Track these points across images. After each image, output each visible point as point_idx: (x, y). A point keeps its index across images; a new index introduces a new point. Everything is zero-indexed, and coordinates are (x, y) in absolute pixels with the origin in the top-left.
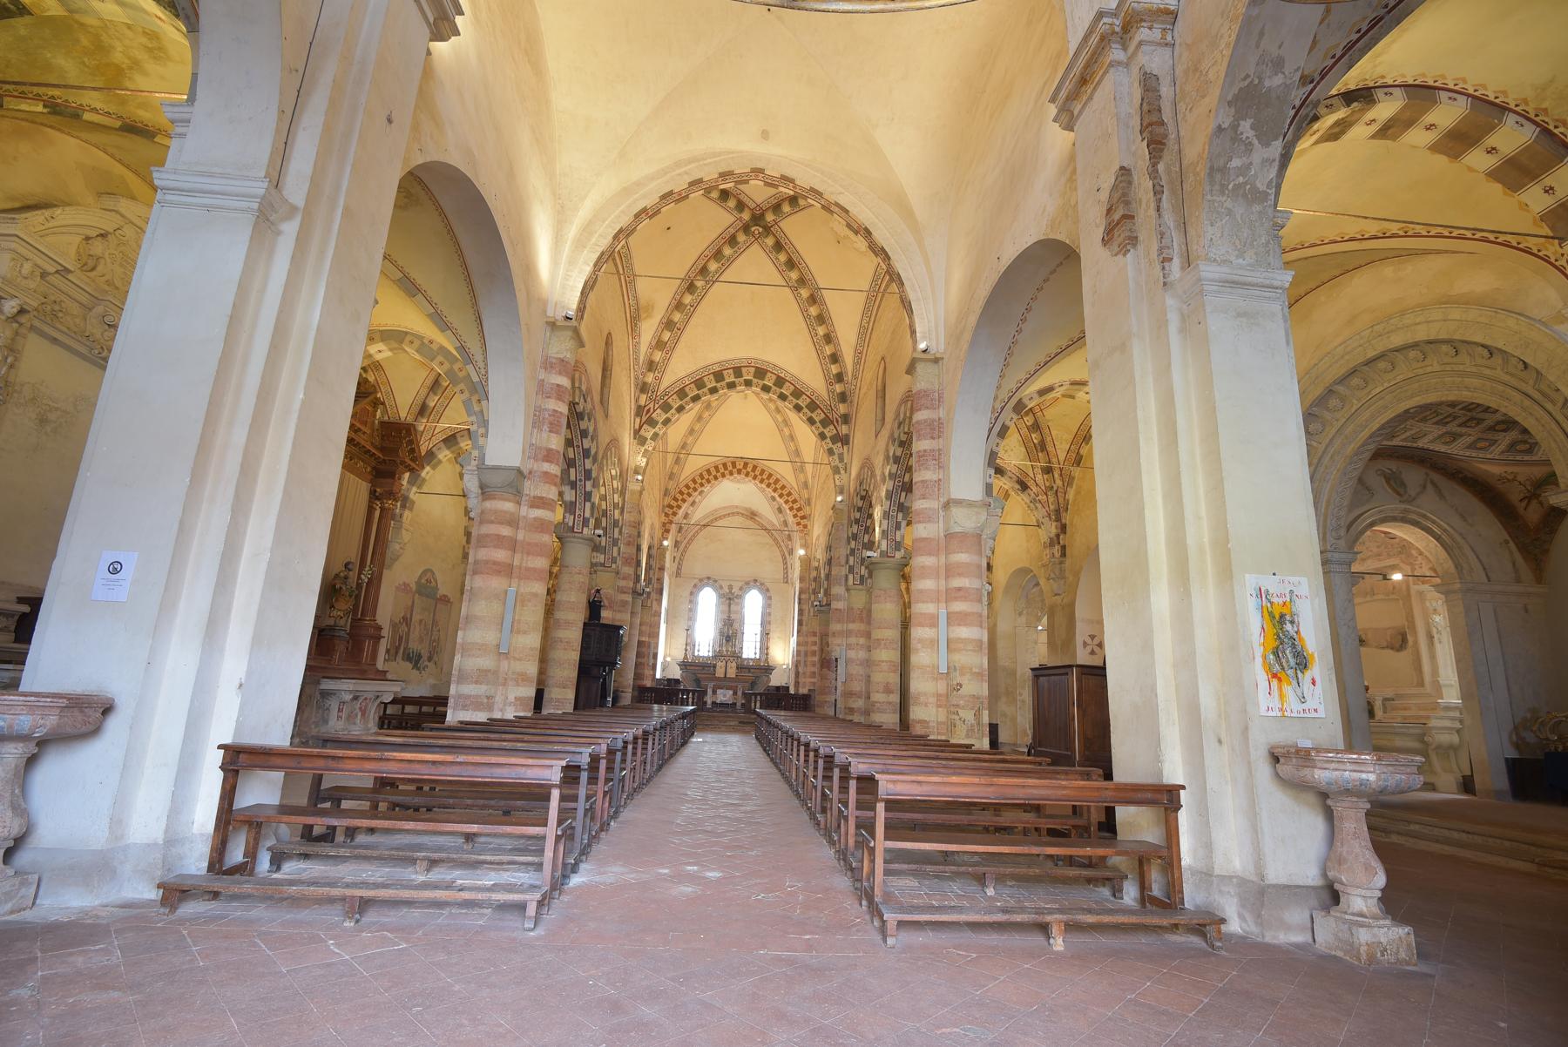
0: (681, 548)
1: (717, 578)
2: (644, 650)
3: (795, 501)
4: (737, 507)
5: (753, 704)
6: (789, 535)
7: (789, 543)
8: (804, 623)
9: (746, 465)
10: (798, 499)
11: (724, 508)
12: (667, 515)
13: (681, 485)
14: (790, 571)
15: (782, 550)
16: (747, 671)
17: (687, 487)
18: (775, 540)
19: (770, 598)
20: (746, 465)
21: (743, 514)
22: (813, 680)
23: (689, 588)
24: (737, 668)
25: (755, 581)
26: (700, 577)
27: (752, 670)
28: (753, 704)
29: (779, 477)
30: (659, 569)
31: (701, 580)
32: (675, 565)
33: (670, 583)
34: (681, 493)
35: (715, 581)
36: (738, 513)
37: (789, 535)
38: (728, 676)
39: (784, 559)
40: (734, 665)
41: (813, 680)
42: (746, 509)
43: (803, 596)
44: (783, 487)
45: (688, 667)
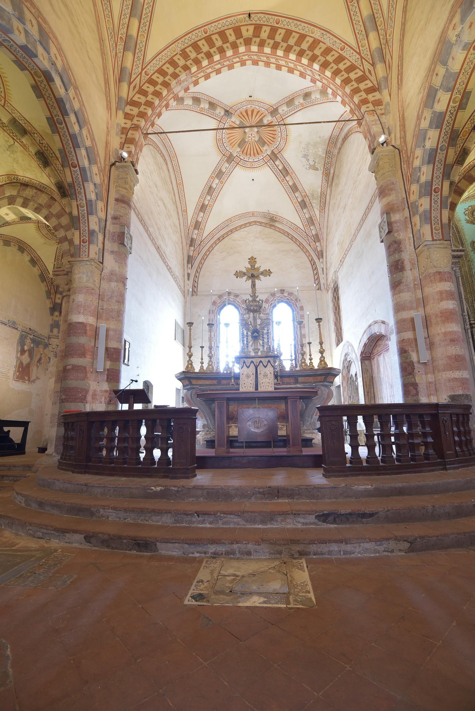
0: (196, 264)
1: (237, 292)
2: (83, 340)
3: (352, 68)
4: (253, 214)
5: (348, 449)
6: (317, 235)
7: (317, 244)
8: (407, 265)
9: (258, 28)
10: (358, 64)
11: (240, 216)
12: (127, 116)
13: (151, 69)
14: (321, 276)
15: (310, 255)
16: (292, 380)
17: (161, 72)
18: (300, 245)
19: (302, 308)
20: (258, 28)
21: (259, 222)
22: (457, 374)
23: (208, 305)
24: (276, 377)
25: (282, 291)
26: (220, 293)
27: (300, 379)
28: (348, 449)
29: (317, 34)
30: (117, 200)
31: (220, 296)
32: (190, 283)
33: (185, 302)
34: (152, 82)
35: (237, 296)
36: (255, 222)
37: (317, 235)
38: (260, 389)
39: (313, 264)
40: (269, 370)
41: (457, 374)
42: (264, 215)
43: (396, 217)
44: (328, 51)
45: (194, 382)
